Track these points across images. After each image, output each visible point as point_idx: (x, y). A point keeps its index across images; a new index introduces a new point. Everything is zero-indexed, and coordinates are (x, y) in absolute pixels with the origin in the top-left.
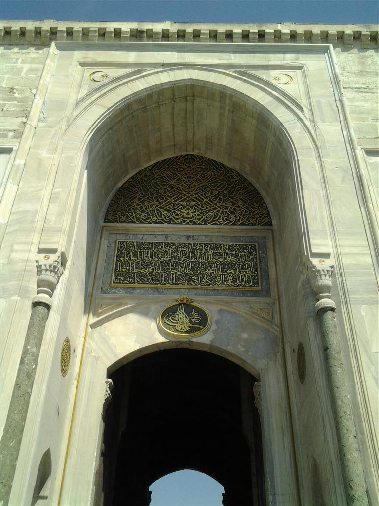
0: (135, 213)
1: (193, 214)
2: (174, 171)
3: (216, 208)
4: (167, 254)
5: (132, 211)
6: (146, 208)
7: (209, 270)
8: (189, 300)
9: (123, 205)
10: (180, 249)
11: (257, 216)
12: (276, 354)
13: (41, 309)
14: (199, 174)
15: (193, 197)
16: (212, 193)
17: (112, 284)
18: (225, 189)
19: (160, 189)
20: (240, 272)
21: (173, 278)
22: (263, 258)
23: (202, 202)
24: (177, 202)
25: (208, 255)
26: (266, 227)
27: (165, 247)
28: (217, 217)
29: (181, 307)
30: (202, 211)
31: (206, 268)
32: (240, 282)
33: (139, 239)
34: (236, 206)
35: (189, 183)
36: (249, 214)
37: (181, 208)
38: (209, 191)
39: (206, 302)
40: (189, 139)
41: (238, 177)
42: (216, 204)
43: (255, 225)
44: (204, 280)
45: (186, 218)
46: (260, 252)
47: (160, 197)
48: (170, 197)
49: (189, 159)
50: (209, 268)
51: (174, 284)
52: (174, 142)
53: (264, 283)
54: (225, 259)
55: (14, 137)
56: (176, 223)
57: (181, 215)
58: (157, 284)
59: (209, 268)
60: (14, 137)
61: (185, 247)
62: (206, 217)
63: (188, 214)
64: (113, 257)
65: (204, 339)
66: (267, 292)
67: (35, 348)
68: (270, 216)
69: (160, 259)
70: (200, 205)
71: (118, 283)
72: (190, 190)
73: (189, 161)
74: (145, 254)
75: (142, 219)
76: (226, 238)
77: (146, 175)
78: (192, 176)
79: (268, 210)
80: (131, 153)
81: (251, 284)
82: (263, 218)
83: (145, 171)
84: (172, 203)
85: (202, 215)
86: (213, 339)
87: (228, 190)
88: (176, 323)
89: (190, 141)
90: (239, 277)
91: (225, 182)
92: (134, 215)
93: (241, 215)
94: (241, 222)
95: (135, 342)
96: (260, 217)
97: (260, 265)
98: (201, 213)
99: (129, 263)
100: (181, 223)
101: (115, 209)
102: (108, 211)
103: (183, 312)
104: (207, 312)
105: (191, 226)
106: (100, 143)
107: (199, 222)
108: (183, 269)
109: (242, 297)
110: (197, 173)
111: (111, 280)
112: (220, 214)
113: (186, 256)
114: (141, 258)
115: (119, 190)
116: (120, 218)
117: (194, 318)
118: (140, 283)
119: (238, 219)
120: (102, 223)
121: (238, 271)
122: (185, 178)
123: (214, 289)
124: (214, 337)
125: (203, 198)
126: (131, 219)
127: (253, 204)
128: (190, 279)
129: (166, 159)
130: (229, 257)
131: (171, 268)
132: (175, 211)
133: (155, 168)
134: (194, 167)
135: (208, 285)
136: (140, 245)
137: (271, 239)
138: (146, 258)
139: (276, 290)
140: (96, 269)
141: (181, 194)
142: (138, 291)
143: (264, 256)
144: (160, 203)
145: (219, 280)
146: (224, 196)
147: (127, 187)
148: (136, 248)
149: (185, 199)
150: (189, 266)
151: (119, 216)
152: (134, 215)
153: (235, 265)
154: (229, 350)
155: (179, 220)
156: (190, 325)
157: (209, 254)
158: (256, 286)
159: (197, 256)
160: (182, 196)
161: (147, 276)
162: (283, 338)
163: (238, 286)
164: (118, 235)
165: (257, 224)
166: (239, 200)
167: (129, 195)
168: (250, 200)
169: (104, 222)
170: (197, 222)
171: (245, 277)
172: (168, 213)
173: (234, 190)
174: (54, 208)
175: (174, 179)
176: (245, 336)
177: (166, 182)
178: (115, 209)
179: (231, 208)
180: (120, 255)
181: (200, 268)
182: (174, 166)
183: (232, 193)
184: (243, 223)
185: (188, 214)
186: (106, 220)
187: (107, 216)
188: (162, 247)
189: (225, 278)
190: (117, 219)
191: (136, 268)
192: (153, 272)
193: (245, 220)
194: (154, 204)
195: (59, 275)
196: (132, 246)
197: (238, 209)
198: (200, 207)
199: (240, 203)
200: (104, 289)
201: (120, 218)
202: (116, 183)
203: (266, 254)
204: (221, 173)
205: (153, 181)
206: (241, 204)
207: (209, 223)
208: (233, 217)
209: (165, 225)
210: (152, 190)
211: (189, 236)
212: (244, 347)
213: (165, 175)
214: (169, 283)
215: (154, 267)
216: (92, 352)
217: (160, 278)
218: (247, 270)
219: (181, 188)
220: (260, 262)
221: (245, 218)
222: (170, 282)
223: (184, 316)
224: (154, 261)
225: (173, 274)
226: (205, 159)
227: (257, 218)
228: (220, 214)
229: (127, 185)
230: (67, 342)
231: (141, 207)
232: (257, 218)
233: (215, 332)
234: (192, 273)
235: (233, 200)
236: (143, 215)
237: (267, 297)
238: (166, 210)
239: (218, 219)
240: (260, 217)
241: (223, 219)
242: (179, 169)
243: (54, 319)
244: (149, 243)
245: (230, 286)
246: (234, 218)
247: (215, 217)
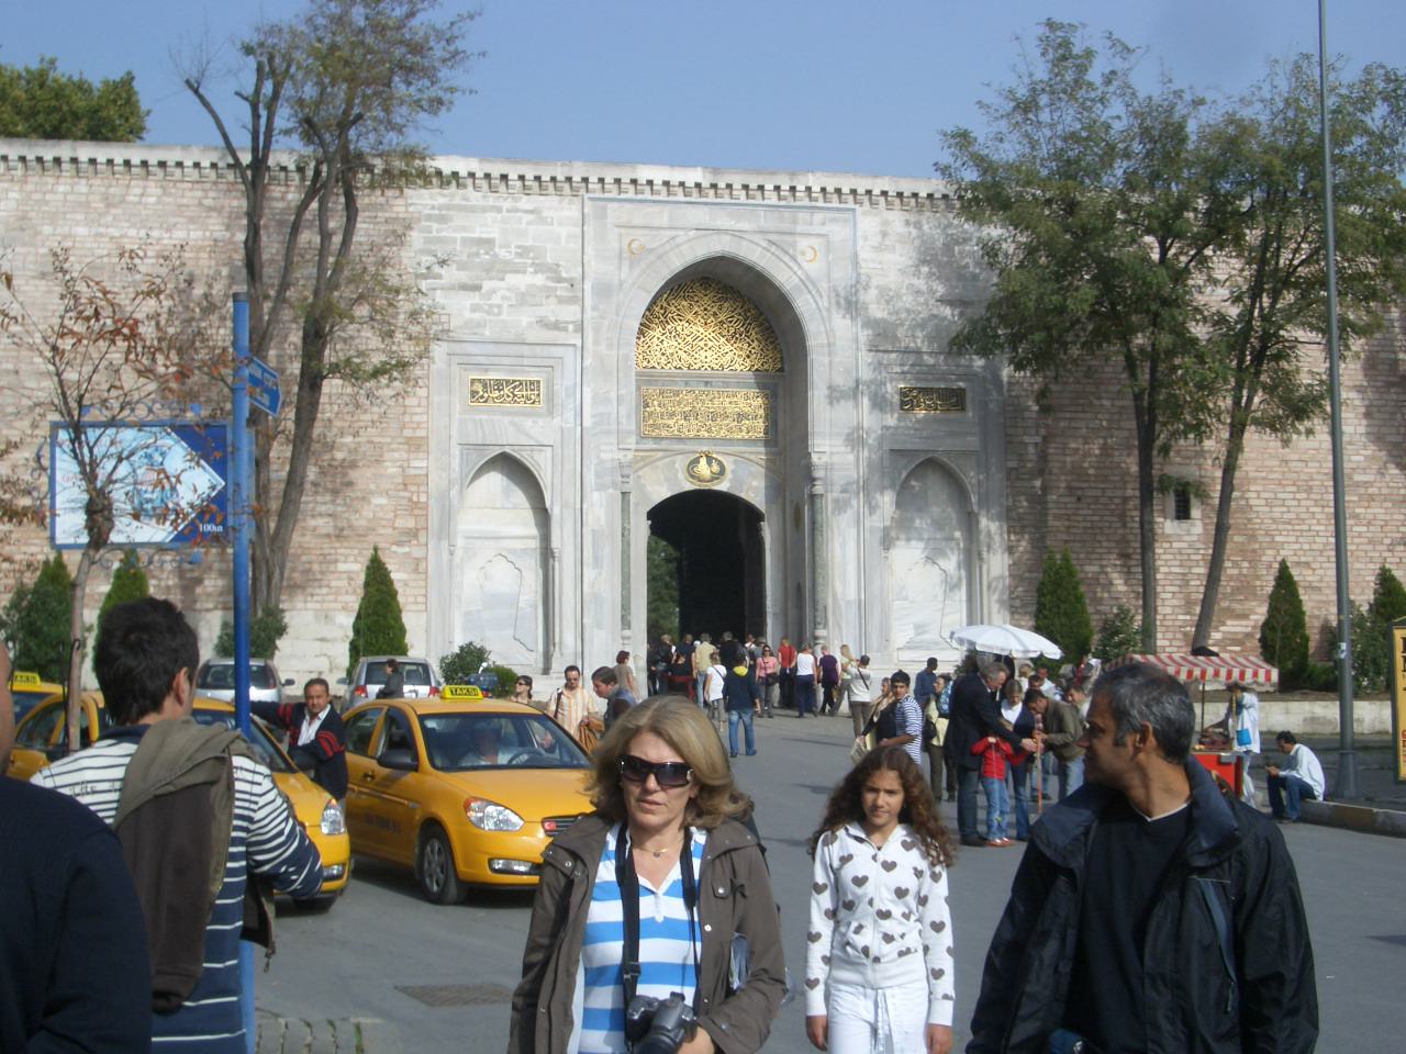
55: (575, 331)
60: (575, 331)
65: (723, 486)
174: (623, 411)
199: (755, 344)
233: (731, 481)
236: (664, 358)
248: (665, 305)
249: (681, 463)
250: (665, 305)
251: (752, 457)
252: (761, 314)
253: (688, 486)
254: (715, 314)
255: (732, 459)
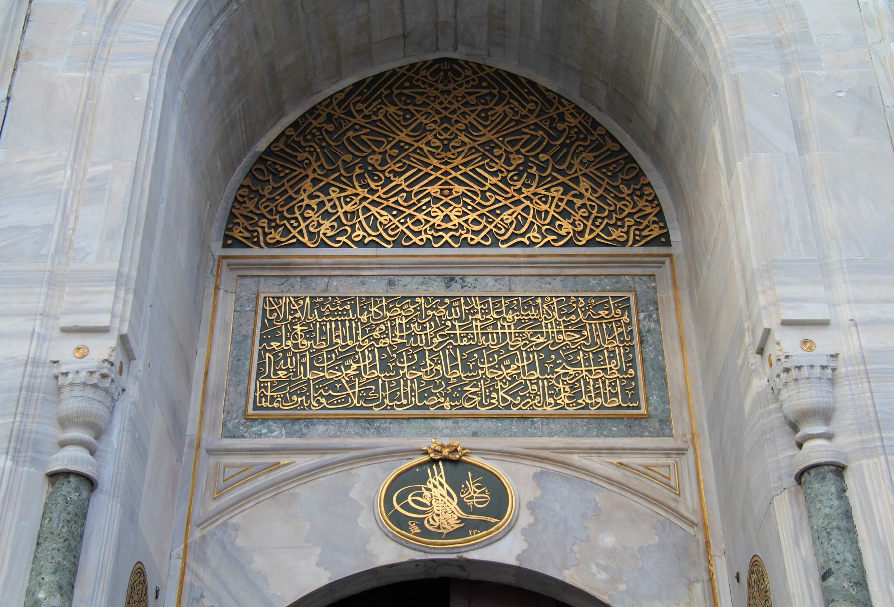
0: (305, 219)
1: (461, 220)
2: (406, 104)
3: (517, 203)
4: (393, 327)
5: (297, 214)
6: (334, 206)
7: (507, 367)
8: (456, 450)
9: (273, 200)
10: (429, 313)
11: (629, 221)
12: (690, 585)
13: (68, 489)
14: (473, 111)
15: (458, 175)
16: (508, 162)
17: (251, 411)
18: (544, 151)
19: (370, 154)
20: (589, 371)
21: (412, 390)
22: (649, 331)
23: (485, 186)
24: (416, 188)
25: (503, 327)
26: (654, 250)
27: (389, 310)
28: (523, 226)
29: (438, 467)
30: (484, 211)
31: (500, 362)
32: (590, 398)
33: (318, 288)
34: (574, 196)
35: (446, 136)
36: (609, 216)
37: (427, 204)
38: (502, 155)
39: (503, 454)
40: (442, 19)
41: (575, 118)
42: (519, 191)
43: (624, 244)
44: (494, 395)
45: (444, 230)
46: (642, 316)
47: (372, 175)
48: (397, 174)
49: (446, 70)
50: (507, 362)
51: (416, 407)
52: (404, 27)
53: (654, 399)
54: (548, 338)
56: (415, 245)
57: (427, 221)
58: (371, 408)
59: (507, 362)
61: (441, 308)
62: (495, 226)
63: (447, 218)
64: (250, 341)
65: (505, 550)
66: (661, 421)
67: (58, 595)
68: (664, 221)
69: (377, 341)
70: (477, 195)
71: (267, 408)
72: (449, 155)
73: (446, 76)
74: (337, 328)
75: (325, 234)
76: (548, 279)
77: (330, 117)
78: (455, 117)
79: (659, 205)
80: (290, 58)
81: (618, 402)
82: (647, 226)
83: (327, 106)
84: (403, 190)
85: (484, 222)
86: (524, 552)
87: (551, 152)
88: (424, 512)
89: (446, 22)
90: (587, 384)
91: (541, 132)
92: (303, 225)
93: (587, 218)
94: (587, 237)
95: (318, 565)
96: (637, 223)
97: (642, 353)
98: (481, 215)
99: (295, 354)
100: (428, 244)
101: (251, 211)
102: (232, 215)
103: (443, 481)
104: (506, 480)
105: (456, 250)
106: (208, 38)
107: (477, 239)
108: (439, 367)
109: (598, 436)
110: (467, 110)
111: (247, 402)
112: (530, 218)
113: (446, 332)
114: (326, 340)
115: (261, 160)
116: (266, 235)
117: (472, 498)
118: (324, 408)
119: (581, 228)
120: (217, 249)
121: (583, 368)
122: (435, 122)
123: (524, 418)
124: (525, 546)
125: (486, 175)
126: (294, 237)
127: (617, 188)
128: (456, 393)
129: (383, 74)
130: (560, 332)
131: (406, 365)
132: (411, 211)
133: (354, 98)
134: (460, 92)
135: (507, 408)
136: (322, 305)
137: (670, 281)
138: (340, 341)
139: (686, 415)
140: (206, 373)
141: (427, 165)
142: (321, 428)
143: (652, 325)
144: (372, 191)
145: (536, 394)
146: (541, 169)
147: (282, 150)
148: (312, 312)
149: (437, 179)
150: (454, 358)
151: (263, 228)
152: (303, 225)
153: (577, 353)
154: (568, 580)
155: (424, 236)
156: (464, 515)
157: (505, 324)
158: (633, 408)
159: (475, 332)
160: (428, 170)
161: (343, 389)
162: (707, 543)
163: (586, 407)
164: (262, 280)
165: (630, 243)
166: (581, 178)
167: (287, 171)
168: (608, 177)
169: (225, 246)
170: (472, 240)
171: (604, 383)
172: (395, 216)
173: (566, 154)
175: (406, 127)
176: (608, 540)
177: (387, 136)
178: (251, 211)
179: (561, 200)
180: (270, 334)
181: (483, 363)
182: (406, 92)
183: (561, 161)
184: (594, 238)
185: (447, 218)
186: (229, 241)
187: (231, 230)
188: (381, 308)
189: (551, 387)
190: (258, 237)
191: (313, 367)
192: (359, 375)
193: (598, 231)
194: (356, 195)
195: (116, 397)
196: (302, 309)
197: (578, 202)
198: (478, 200)
199: (584, 185)
200: (230, 425)
201: (266, 235)
202: (251, 142)
203: (657, 321)
204: (531, 106)
205: (351, 133)
206: (586, 190)
207: (503, 242)
208: (565, 223)
209: (389, 249)
210: (348, 158)
211: (452, 278)
212: (605, 569)
213: (381, 117)
214: (402, 405)
215: (361, 364)
216: (202, 596)
217: (377, 391)
218: (608, 366)
219: (426, 148)
220: (641, 342)
221: (598, 226)
222: (404, 402)
223: (444, 493)
224: (360, 347)
225: (412, 380)
226: (488, 70)
227: (629, 226)
228: (530, 218)
229: (281, 144)
230: (139, 572)
231: (321, 204)
232: (629, 226)
233: (527, 533)
234: (463, 375)
235: (565, 180)
236: (327, 224)
237: (664, 435)
238: (388, 208)
239: (527, 231)
240: (637, 223)
241: (540, 232)
242: (419, 100)
243: (105, 515)
244: (345, 300)
245: (563, 408)
246: (570, 226)
247: (519, 226)
248: (338, 113)
249: (371, 483)
250: (338, 113)
251: (595, 463)
252: (596, 124)
253: (387, 552)
254: (469, 129)
255: (528, 469)
